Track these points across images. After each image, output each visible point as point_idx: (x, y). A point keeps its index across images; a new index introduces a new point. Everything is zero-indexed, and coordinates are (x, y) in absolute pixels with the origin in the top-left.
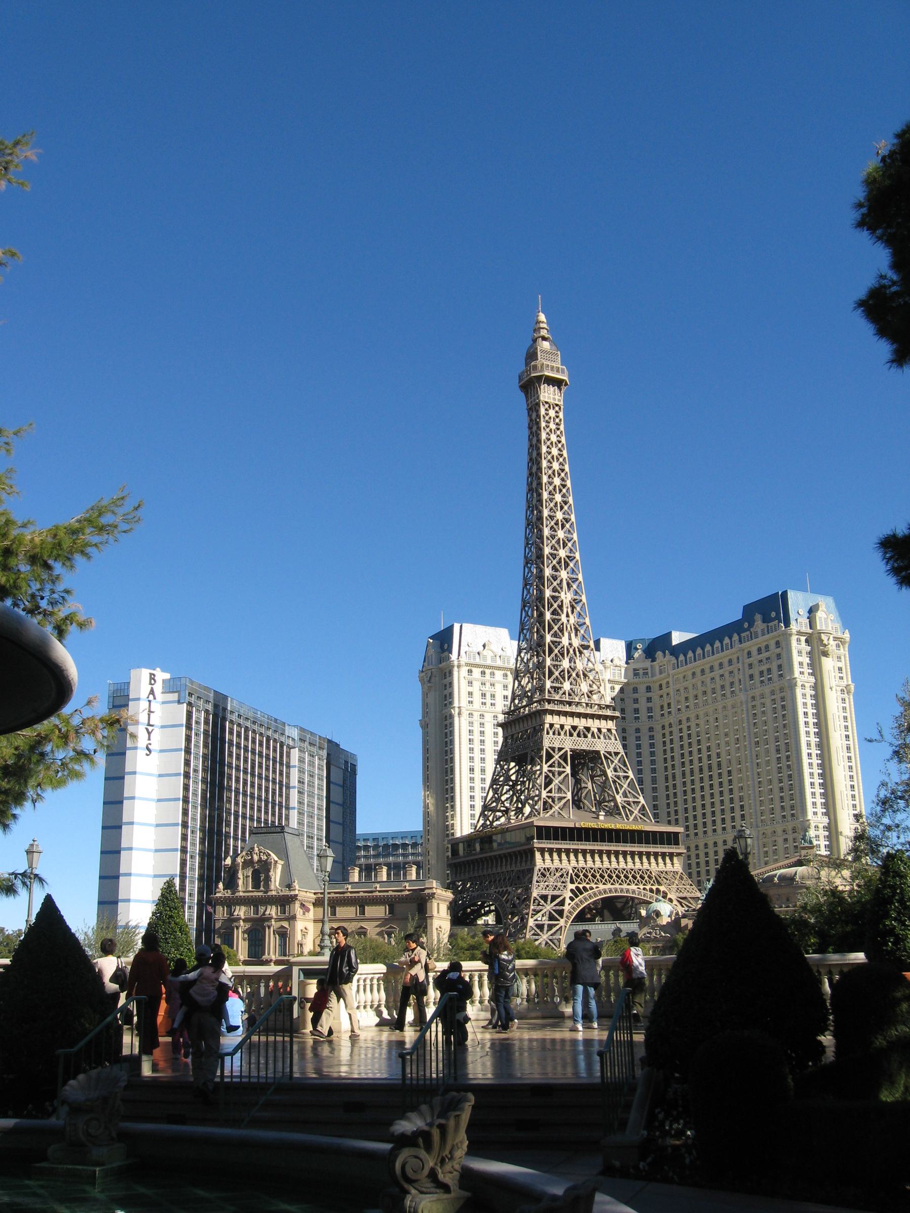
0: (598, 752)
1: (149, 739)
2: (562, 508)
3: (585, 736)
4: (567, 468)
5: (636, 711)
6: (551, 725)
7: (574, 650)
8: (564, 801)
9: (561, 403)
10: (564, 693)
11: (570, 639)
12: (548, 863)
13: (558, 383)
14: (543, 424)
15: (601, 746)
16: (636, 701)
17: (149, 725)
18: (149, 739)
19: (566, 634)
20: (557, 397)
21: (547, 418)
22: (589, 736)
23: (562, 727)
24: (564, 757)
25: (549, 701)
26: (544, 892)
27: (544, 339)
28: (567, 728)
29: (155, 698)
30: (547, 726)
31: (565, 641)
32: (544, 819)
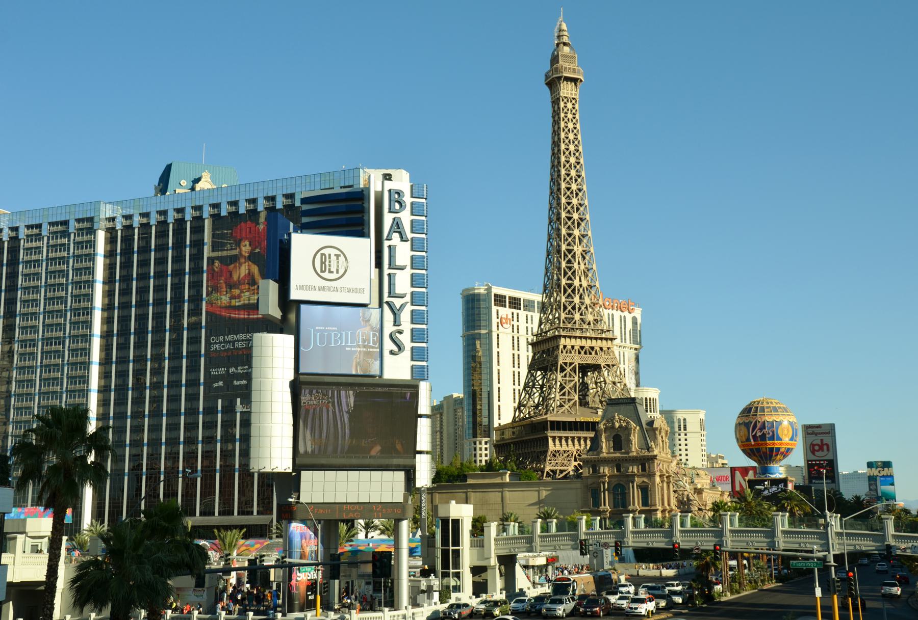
2: (576, 180)
3: (590, 354)
4: (580, 149)
8: (572, 402)
9: (577, 97)
10: (575, 323)
11: (580, 280)
12: (558, 447)
13: (575, 81)
14: (562, 115)
15: (601, 360)
20: (573, 92)
21: (566, 110)
22: (593, 353)
23: (573, 347)
25: (564, 329)
26: (554, 468)
27: (565, 44)
28: (576, 348)
30: (561, 347)
31: (576, 283)
32: (557, 415)
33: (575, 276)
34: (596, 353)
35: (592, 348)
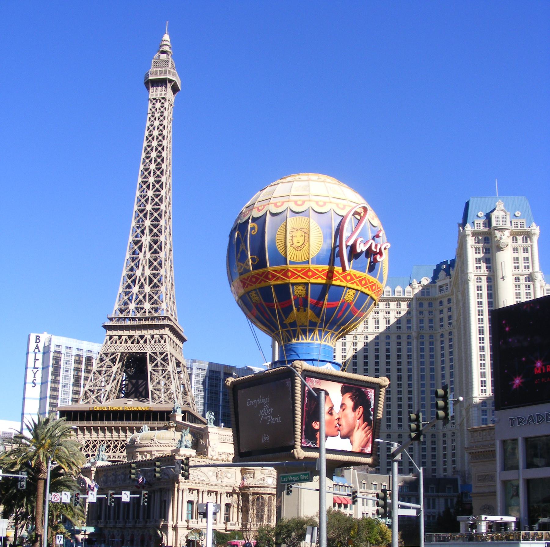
0: (146, 353)
1: (35, 377)
3: (138, 342)
5: (441, 320)
6: (111, 337)
7: (145, 279)
11: (143, 270)
15: (148, 349)
16: (441, 312)
17: (34, 368)
18: (35, 377)
19: (141, 268)
22: (142, 342)
23: (120, 337)
24: (113, 361)
29: (39, 351)
31: (138, 273)
33: (138, 267)
34: (145, 342)
35: (142, 337)
